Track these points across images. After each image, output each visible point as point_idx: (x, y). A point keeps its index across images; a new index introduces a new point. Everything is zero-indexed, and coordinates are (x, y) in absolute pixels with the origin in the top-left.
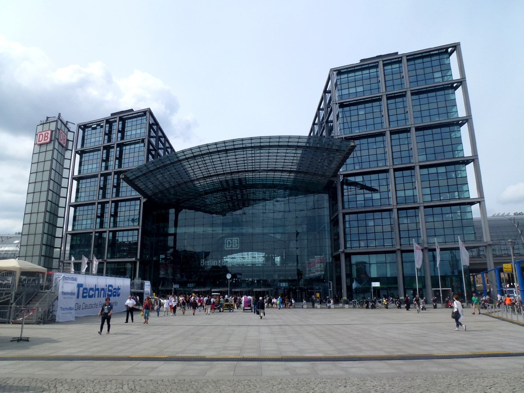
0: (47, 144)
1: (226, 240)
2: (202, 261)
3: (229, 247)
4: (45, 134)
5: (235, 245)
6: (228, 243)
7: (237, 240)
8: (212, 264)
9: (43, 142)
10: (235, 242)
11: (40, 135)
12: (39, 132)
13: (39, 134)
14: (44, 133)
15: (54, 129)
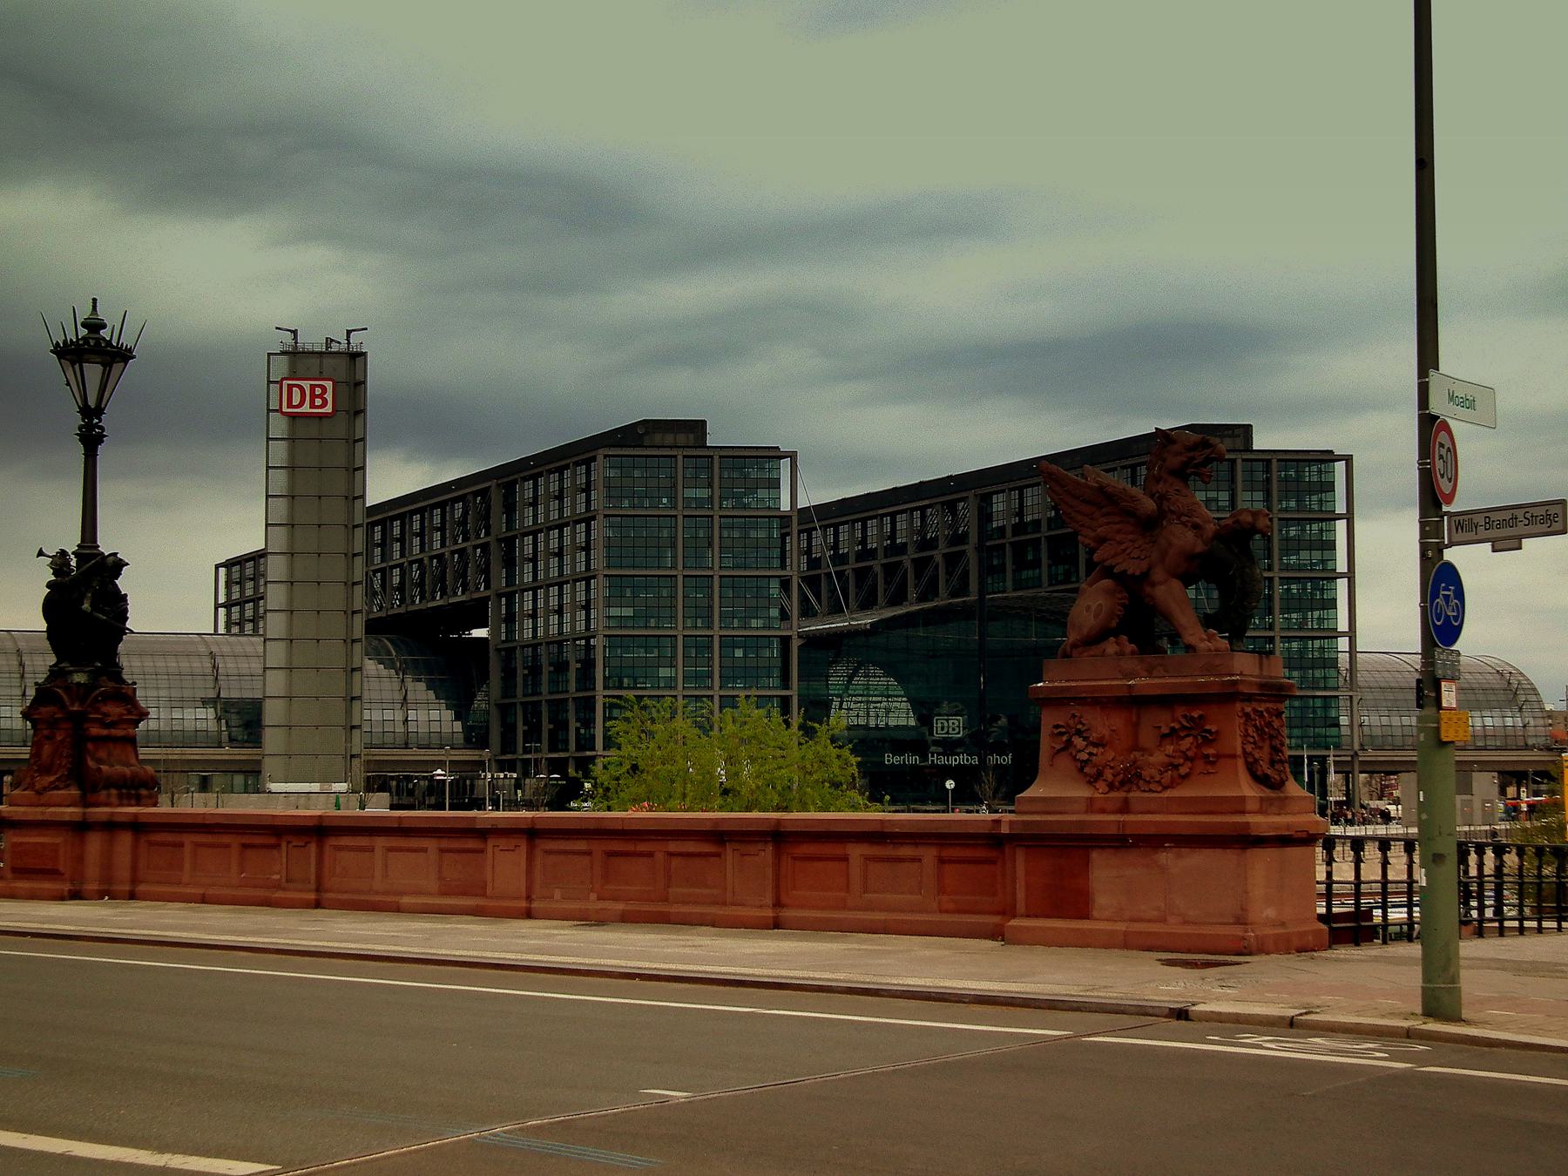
0: (321, 416)
1: (937, 720)
2: (888, 756)
3: (946, 730)
4: (313, 387)
5: (954, 729)
6: (939, 725)
7: (959, 721)
8: (908, 761)
9: (306, 408)
10: (953, 723)
11: (290, 387)
12: (283, 379)
13: (285, 383)
14: (306, 385)
15: (342, 375)
